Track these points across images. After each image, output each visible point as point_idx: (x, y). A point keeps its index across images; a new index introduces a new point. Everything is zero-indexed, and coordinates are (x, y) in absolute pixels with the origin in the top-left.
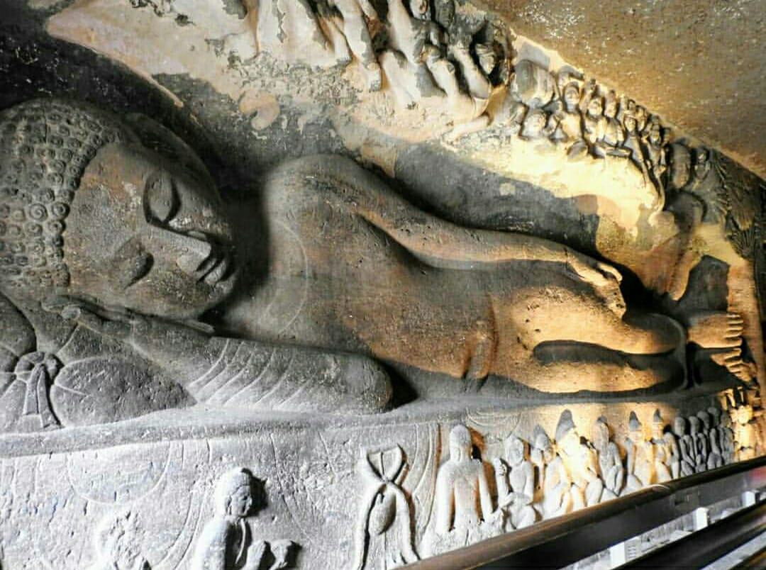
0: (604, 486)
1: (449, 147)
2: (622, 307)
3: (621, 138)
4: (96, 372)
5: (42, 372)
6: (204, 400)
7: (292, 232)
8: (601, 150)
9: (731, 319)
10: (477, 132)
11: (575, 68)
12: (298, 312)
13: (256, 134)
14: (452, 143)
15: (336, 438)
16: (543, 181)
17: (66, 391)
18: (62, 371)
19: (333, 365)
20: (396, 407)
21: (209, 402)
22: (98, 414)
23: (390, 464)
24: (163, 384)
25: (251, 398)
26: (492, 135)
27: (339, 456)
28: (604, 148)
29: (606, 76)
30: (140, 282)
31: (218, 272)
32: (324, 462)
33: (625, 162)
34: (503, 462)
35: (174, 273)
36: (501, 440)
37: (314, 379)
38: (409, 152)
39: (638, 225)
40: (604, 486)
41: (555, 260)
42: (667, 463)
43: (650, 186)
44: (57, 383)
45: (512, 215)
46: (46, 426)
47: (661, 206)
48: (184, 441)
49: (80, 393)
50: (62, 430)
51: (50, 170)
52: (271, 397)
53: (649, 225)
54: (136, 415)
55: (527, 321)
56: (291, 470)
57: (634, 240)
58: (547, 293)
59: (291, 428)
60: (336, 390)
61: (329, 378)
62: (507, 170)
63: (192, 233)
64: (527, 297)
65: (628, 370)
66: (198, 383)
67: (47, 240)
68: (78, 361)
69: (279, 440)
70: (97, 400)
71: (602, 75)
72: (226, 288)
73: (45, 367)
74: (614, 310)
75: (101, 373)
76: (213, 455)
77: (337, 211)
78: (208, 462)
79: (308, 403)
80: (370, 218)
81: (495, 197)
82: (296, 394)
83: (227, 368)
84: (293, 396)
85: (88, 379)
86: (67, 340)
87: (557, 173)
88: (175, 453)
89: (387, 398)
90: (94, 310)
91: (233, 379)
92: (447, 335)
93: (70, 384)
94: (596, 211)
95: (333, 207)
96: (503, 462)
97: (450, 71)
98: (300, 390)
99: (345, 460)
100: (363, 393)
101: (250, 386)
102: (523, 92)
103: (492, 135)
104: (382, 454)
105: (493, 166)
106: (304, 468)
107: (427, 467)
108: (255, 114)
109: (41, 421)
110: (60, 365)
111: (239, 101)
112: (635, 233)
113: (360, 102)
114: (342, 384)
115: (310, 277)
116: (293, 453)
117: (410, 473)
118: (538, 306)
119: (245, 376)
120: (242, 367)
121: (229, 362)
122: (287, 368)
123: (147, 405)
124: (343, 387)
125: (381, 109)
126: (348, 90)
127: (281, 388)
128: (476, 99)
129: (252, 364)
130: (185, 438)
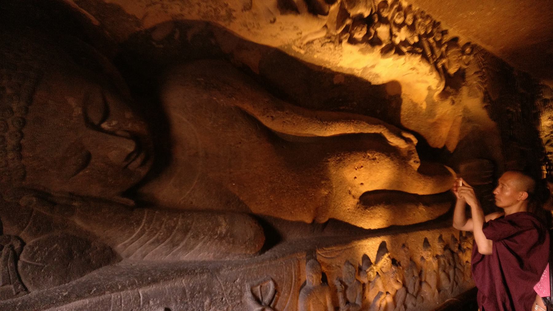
0: (407, 292)
1: (297, 50)
2: (417, 162)
3: (416, 39)
4: (51, 246)
5: (11, 252)
6: (128, 256)
8: (405, 50)
13: (154, 43)
14: (300, 48)
15: (229, 278)
16: (363, 72)
17: (30, 264)
18: (26, 247)
19: (224, 224)
20: (268, 250)
21: (131, 258)
22: (54, 280)
23: (267, 293)
24: (98, 249)
25: (164, 252)
26: (329, 40)
27: (231, 291)
28: (405, 47)
30: (81, 173)
31: (139, 161)
32: (221, 297)
33: (419, 57)
34: (341, 282)
36: (339, 267)
37: (211, 236)
40: (407, 292)
41: (373, 132)
42: (446, 271)
43: (435, 74)
44: (22, 258)
46: (18, 293)
47: (442, 87)
48: (122, 293)
49: (40, 264)
50: (29, 294)
51: (9, 91)
52: (179, 251)
54: (82, 276)
55: (355, 178)
56: (198, 305)
58: (369, 157)
59: (197, 274)
60: (227, 242)
61: (221, 233)
62: (339, 65)
63: (119, 133)
64: (355, 160)
65: (422, 208)
66: (125, 245)
67: (9, 147)
68: (38, 239)
69: (189, 284)
70: (54, 268)
72: (143, 172)
73: (12, 247)
74: (412, 165)
75: (55, 246)
76: (143, 300)
77: (222, 105)
78: (139, 306)
79: (206, 253)
80: (245, 108)
82: (197, 247)
83: (146, 233)
84: (195, 249)
85: (45, 252)
86: (27, 224)
87: (373, 67)
88: (116, 302)
89: (262, 244)
90: (44, 197)
91: (151, 240)
93: (32, 258)
95: (218, 102)
96: (341, 282)
98: (200, 244)
99: (235, 294)
100: (245, 243)
101: (163, 244)
102: (352, 8)
103: (329, 40)
104: (261, 287)
106: (207, 302)
107: (291, 292)
109: (13, 290)
110: (23, 244)
112: (424, 106)
113: (234, 18)
114: (231, 237)
116: (199, 292)
117: (280, 298)
118: (362, 167)
119: (160, 237)
120: (157, 231)
121: (149, 228)
122: (190, 229)
123: (89, 267)
124: (231, 239)
125: (250, 24)
127: (186, 244)
128: (319, 16)
129: (166, 228)
130: (122, 290)
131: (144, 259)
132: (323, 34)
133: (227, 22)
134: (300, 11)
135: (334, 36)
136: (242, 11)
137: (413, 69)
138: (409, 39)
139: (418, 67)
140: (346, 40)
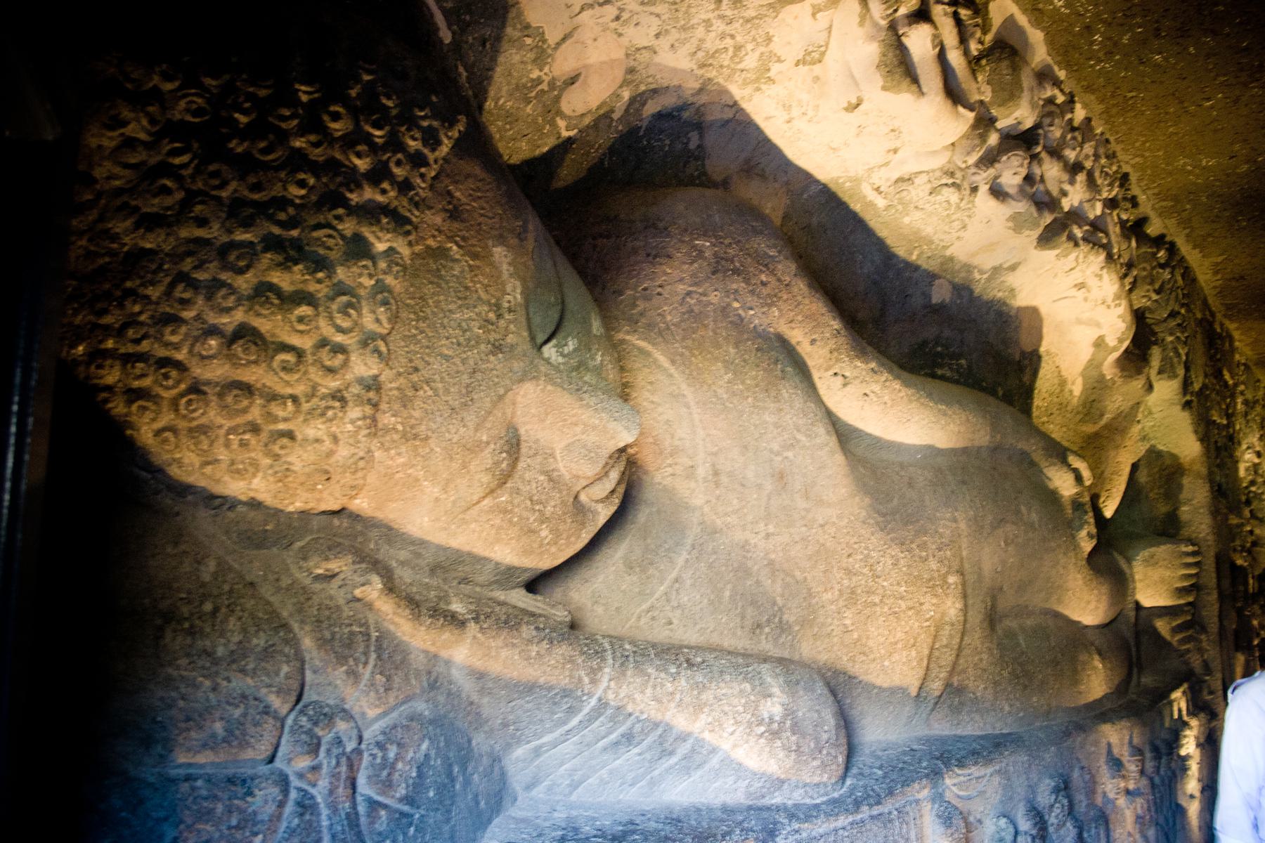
1: (871, 195)
3: (1098, 209)
6: (529, 787)
7: (672, 370)
8: (1078, 233)
9: (1188, 554)
10: (928, 172)
11: (1056, 68)
12: (680, 561)
14: (877, 189)
16: (989, 280)
21: (538, 792)
26: (950, 181)
28: (1080, 227)
29: (1093, 92)
33: (1102, 257)
35: (551, 480)
38: (805, 196)
39: (1083, 374)
45: (942, 346)
53: (1103, 376)
57: (1075, 401)
60: (784, 747)
62: (948, 253)
71: (1089, 89)
74: (1083, 544)
81: (925, 307)
84: (707, 767)
91: (613, 737)
92: (910, 609)
94: (1039, 345)
97: (934, 47)
101: (636, 750)
105: (931, 242)
108: (572, 81)
111: (558, 44)
112: (1077, 388)
115: (705, 480)
124: (794, 738)
126: (762, 54)
128: (961, 109)
131: (573, 798)
132: (940, 161)
133: (748, 90)
134: (925, 90)
135: (961, 169)
136: (797, 65)
137: (1081, 286)
138: (1086, 206)
139: (1093, 282)
140: (988, 187)
